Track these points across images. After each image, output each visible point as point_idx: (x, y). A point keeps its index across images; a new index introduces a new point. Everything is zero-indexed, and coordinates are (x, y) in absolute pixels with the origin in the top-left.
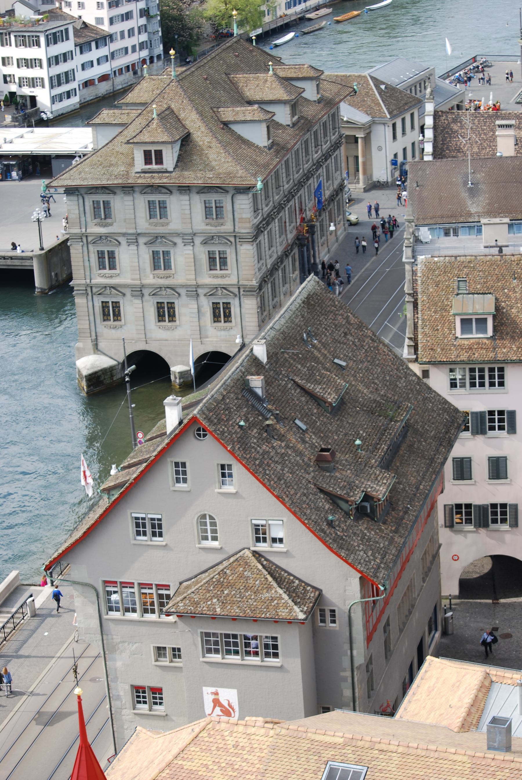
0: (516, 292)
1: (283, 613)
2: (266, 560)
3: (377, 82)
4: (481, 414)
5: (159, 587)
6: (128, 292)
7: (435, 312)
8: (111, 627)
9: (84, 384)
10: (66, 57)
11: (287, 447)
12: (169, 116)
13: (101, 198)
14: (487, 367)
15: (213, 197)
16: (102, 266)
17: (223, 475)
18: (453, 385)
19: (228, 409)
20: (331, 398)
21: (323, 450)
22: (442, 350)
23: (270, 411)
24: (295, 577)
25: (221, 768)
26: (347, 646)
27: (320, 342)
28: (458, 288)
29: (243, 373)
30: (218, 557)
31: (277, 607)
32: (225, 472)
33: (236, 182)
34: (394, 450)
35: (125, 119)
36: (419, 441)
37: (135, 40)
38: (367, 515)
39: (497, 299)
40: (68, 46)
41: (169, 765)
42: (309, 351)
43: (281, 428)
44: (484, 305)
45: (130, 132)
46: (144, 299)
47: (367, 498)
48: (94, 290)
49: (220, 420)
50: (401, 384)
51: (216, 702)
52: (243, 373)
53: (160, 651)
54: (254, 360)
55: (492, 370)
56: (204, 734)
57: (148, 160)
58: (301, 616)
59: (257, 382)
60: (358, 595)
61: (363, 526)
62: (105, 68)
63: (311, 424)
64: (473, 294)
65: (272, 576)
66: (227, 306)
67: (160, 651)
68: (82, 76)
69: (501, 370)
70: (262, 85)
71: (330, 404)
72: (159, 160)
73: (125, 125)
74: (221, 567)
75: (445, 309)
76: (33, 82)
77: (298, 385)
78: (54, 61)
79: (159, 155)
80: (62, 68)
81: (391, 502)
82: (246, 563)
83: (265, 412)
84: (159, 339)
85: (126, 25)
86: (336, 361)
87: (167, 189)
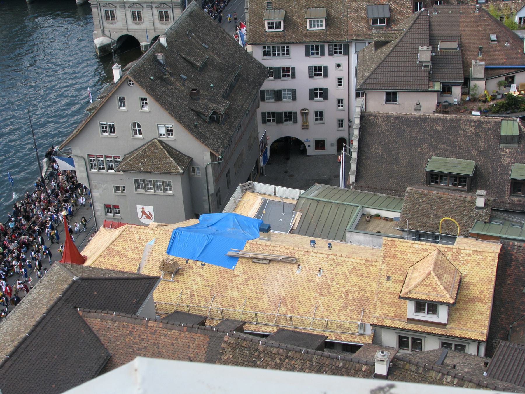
0: (295, 8)
1: (173, 170)
2: (165, 144)
4: (279, 69)
5: (115, 157)
6: (118, 6)
7: (256, 19)
8: (91, 176)
9: (98, 52)
11: (175, 88)
14: (281, 46)
17: (143, 103)
18: (265, 55)
19: (145, 70)
20: (199, 64)
21: (193, 90)
22: (259, 37)
23: (167, 71)
24: (179, 152)
25: (132, 250)
26: (205, 185)
27: (195, 35)
28: (267, 6)
29: (154, 52)
30: (142, 143)
31: (170, 166)
32: (144, 102)
34: (231, 88)
36: (245, 84)
38: (215, 121)
39: (286, 12)
41: (107, 249)
42: (189, 40)
43: (173, 79)
46: (126, 9)
47: (215, 113)
48: (101, 5)
49: (140, 76)
50: (237, 55)
51: (143, 213)
52: (154, 52)
53: (117, 188)
54: (161, 45)
55: (283, 47)
56: (124, 233)
58: (181, 171)
59: (160, 57)
60: (209, 161)
61: (213, 126)
63: (189, 77)
64: (275, 9)
65: (167, 152)
67: (117, 188)
69: (288, 47)
71: (199, 67)
74: (143, 148)
75: (261, 17)
77: (183, 57)
81: (227, 114)
82: (155, 146)
83: (164, 71)
84: (134, 29)
86: (203, 45)
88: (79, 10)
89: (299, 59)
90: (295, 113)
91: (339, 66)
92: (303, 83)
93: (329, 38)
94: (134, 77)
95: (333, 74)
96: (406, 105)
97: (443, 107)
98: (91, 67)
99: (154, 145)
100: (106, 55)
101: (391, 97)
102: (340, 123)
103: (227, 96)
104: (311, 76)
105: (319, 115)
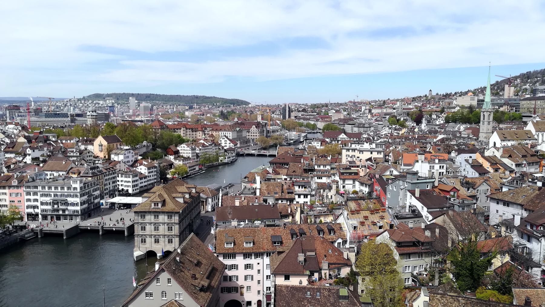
3: (209, 189)
10: (137, 181)
12: (160, 196)
13: (143, 214)
15: (170, 214)
16: (142, 230)
33: (175, 211)
35: (150, 196)
37: (153, 178)
40: (137, 178)
44: (231, 239)
45: (150, 199)
47: (203, 286)
57: (155, 205)
59: (178, 259)
62: (146, 184)
66: (172, 240)
68: (140, 185)
70: (183, 189)
72: (158, 206)
73: (150, 197)
76: (128, 186)
78: (133, 181)
79: (158, 204)
80: (135, 183)
85: (151, 174)
87: (159, 212)
88: (126, 239)
89: (240, 261)
90: (237, 288)
91: (258, 264)
92: (241, 273)
93: (255, 251)
94: (165, 267)
95: (256, 268)
96: (294, 281)
97: (311, 282)
98: (132, 266)
99: (173, 303)
100: (140, 261)
101: (287, 278)
102: (259, 292)
103: (208, 278)
104: (245, 269)
105: (249, 288)
